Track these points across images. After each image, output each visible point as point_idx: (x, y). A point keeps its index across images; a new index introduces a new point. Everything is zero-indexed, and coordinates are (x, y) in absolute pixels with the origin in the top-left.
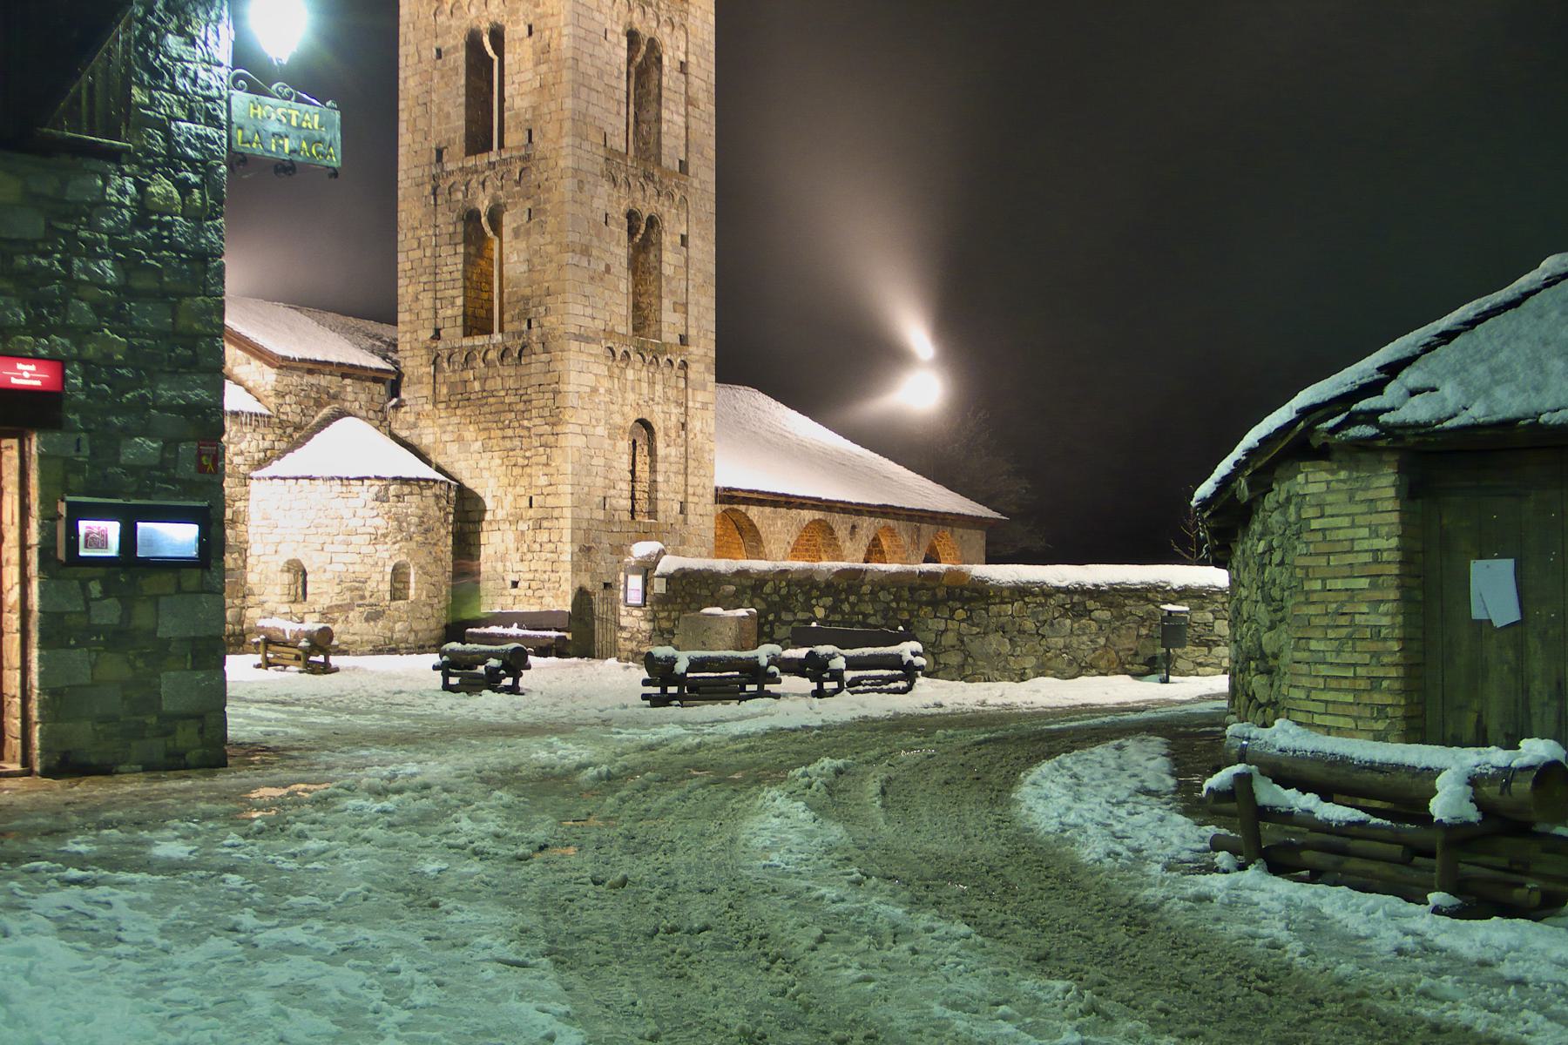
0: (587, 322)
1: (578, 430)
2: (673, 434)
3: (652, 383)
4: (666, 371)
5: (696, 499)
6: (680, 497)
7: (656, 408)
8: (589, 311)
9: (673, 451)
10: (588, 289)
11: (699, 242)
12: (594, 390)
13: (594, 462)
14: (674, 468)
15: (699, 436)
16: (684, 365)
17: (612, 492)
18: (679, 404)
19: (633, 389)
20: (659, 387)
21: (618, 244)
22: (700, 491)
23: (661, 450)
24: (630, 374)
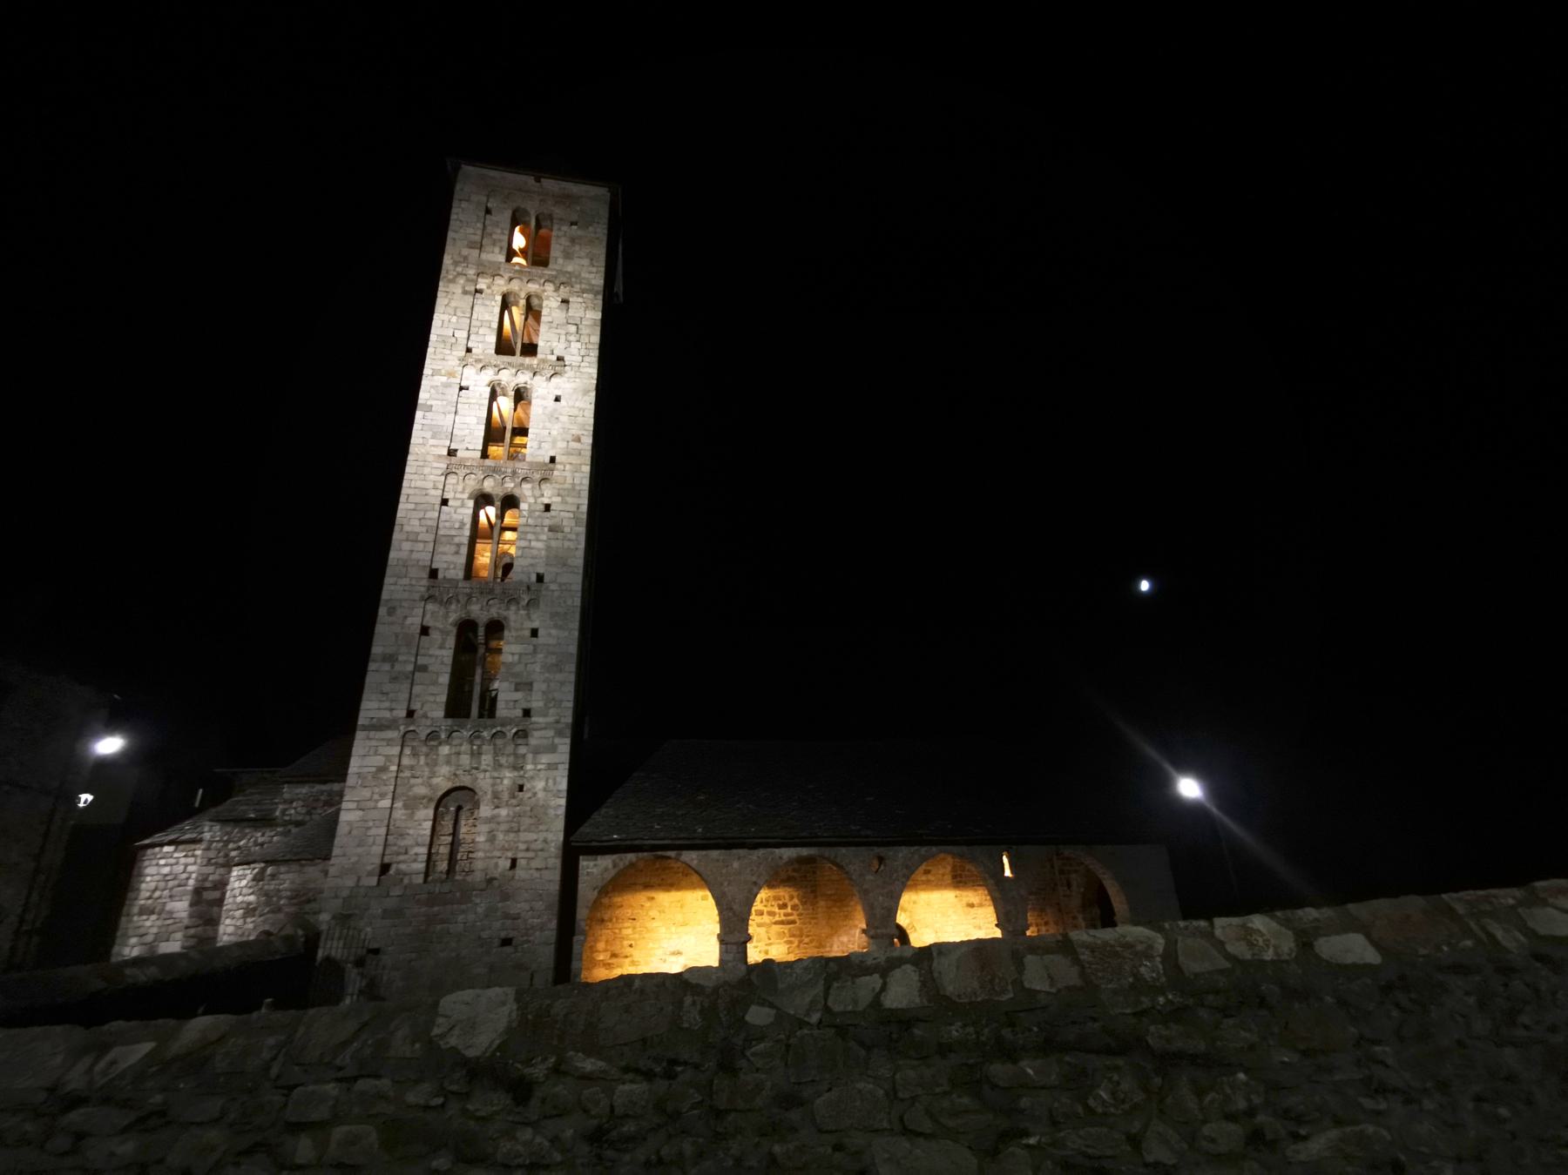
0: (387, 714)
1: (354, 805)
2: (505, 796)
3: (476, 755)
4: (499, 742)
5: (531, 854)
6: (510, 854)
7: (481, 776)
8: (387, 704)
9: (503, 812)
10: (387, 687)
11: (554, 632)
12: (383, 769)
13: (373, 832)
14: (504, 827)
15: (541, 795)
16: (523, 734)
17: (402, 858)
18: (515, 768)
19: (448, 763)
20: (487, 759)
21: (441, 647)
22: (539, 845)
23: (485, 811)
24: (445, 750)
